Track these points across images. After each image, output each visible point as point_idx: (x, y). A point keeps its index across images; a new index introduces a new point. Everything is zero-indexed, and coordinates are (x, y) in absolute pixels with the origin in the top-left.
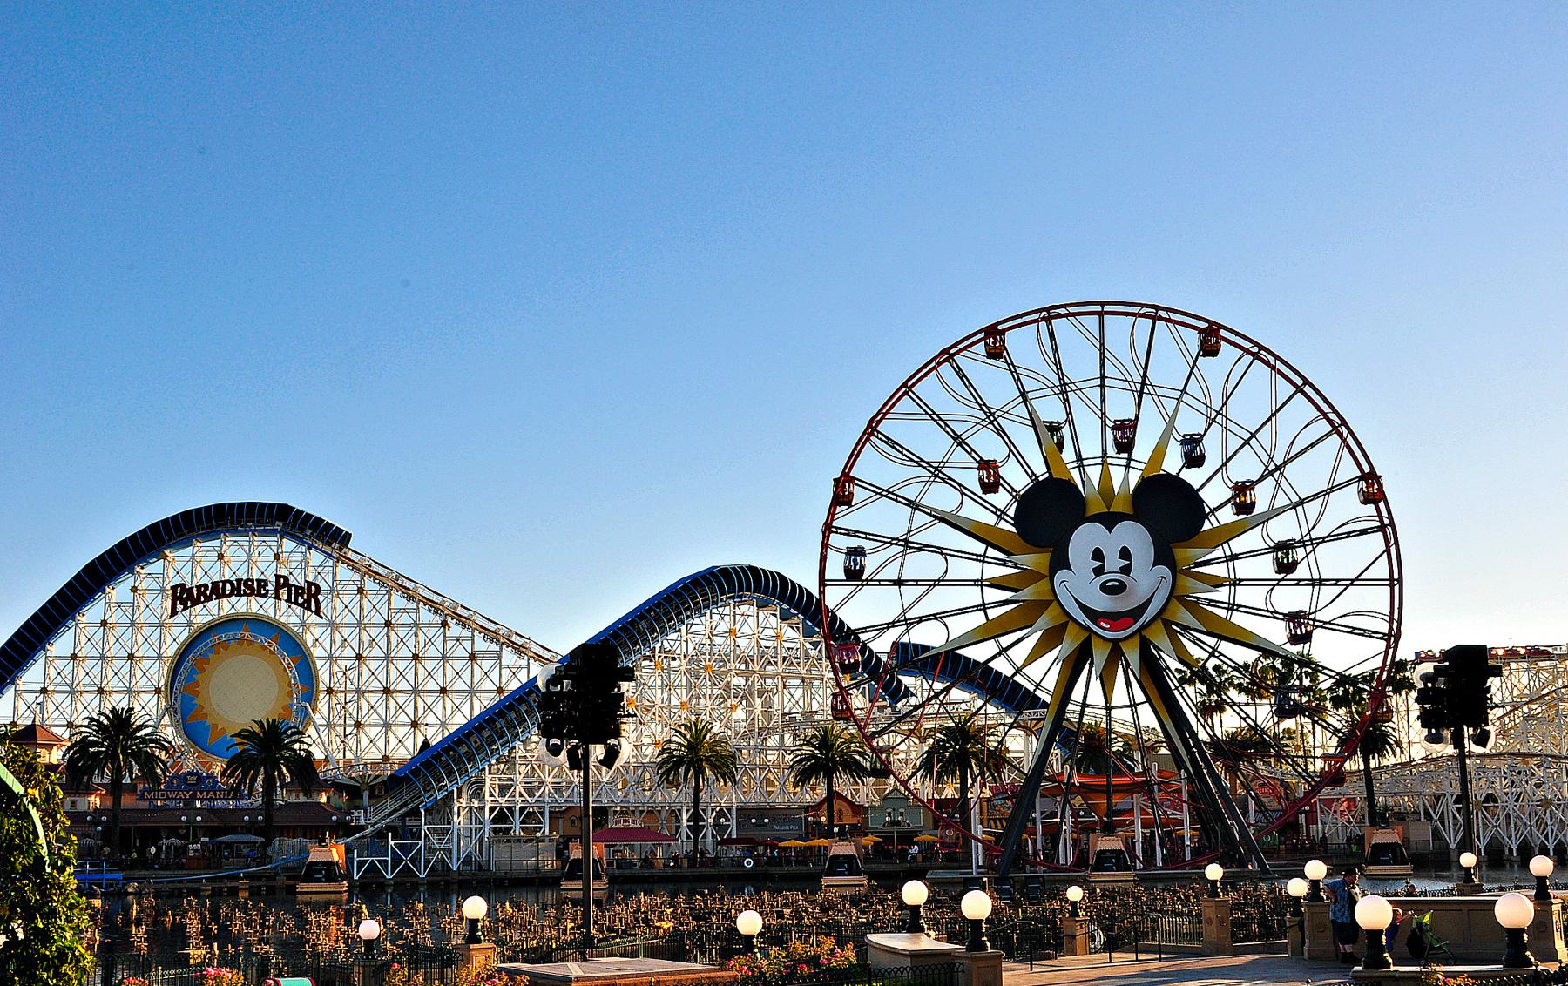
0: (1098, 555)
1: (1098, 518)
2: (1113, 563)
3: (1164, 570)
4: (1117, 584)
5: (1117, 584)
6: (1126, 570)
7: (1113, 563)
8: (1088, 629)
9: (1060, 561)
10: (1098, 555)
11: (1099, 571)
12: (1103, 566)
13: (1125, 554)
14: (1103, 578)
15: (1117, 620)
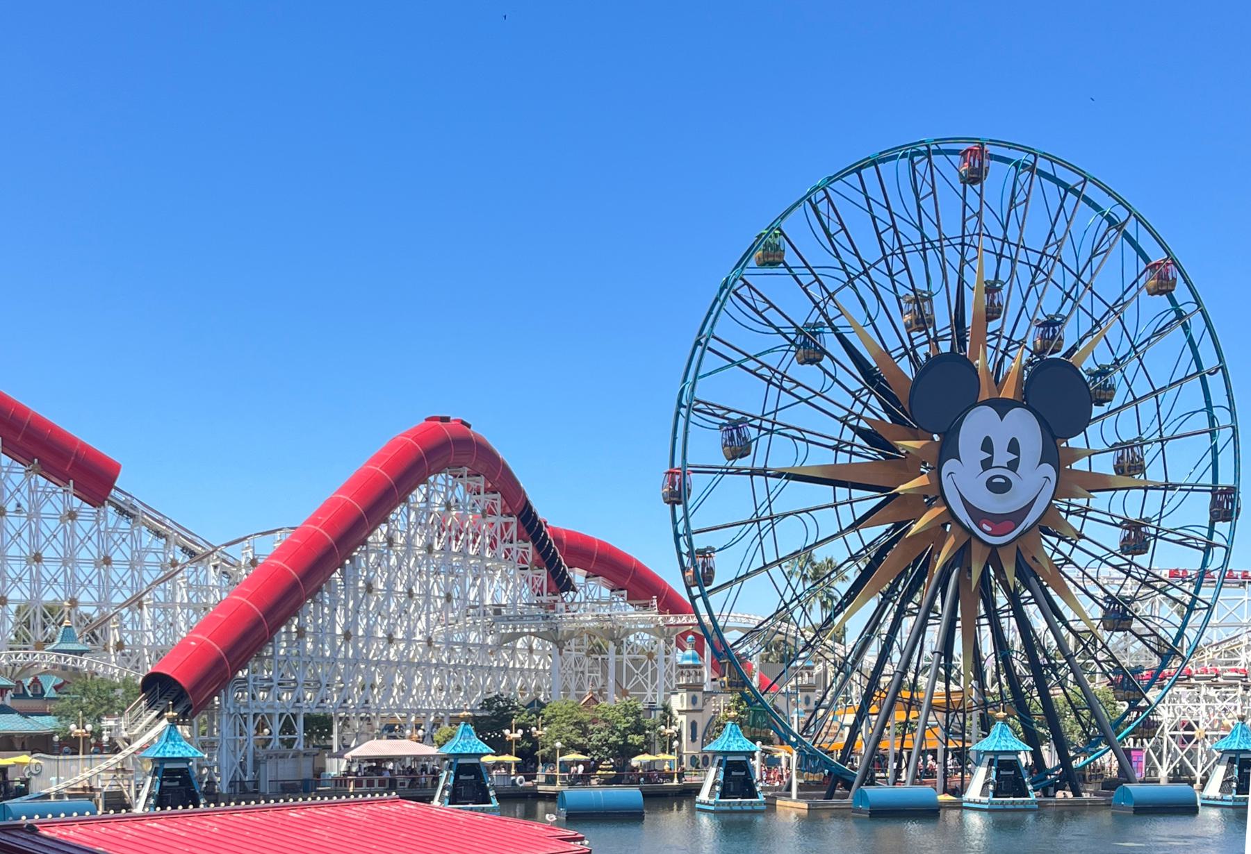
0: (987, 445)
1: (991, 403)
2: (1002, 456)
3: (1049, 470)
4: (1003, 481)
5: (1003, 481)
6: (1013, 466)
7: (1002, 456)
8: (970, 532)
9: (949, 449)
10: (987, 445)
11: (987, 465)
12: (991, 459)
13: (1014, 447)
14: (991, 473)
15: (1002, 522)
